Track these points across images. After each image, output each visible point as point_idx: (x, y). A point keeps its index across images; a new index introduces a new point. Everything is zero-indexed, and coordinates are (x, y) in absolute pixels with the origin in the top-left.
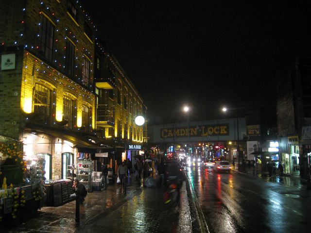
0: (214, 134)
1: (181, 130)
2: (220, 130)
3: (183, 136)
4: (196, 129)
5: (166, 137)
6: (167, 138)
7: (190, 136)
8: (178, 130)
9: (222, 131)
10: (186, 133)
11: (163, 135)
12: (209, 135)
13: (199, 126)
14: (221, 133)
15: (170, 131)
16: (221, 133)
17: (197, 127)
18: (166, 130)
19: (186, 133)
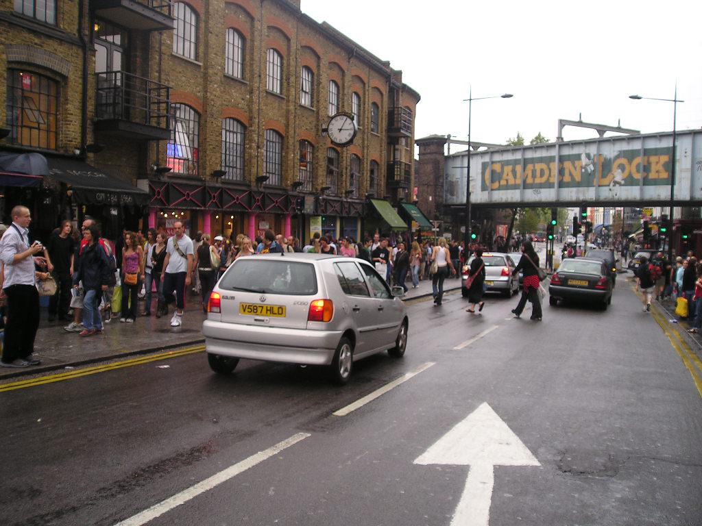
0: (630, 181)
1: (538, 167)
2: (647, 169)
3: (541, 186)
4: (577, 163)
5: (496, 185)
6: (499, 189)
7: (561, 185)
8: (530, 167)
9: (654, 168)
10: (550, 176)
11: (488, 182)
12: (616, 183)
13: (588, 156)
14: (652, 175)
15: (508, 169)
16: (652, 175)
17: (583, 157)
18: (497, 168)
19: (550, 176)
